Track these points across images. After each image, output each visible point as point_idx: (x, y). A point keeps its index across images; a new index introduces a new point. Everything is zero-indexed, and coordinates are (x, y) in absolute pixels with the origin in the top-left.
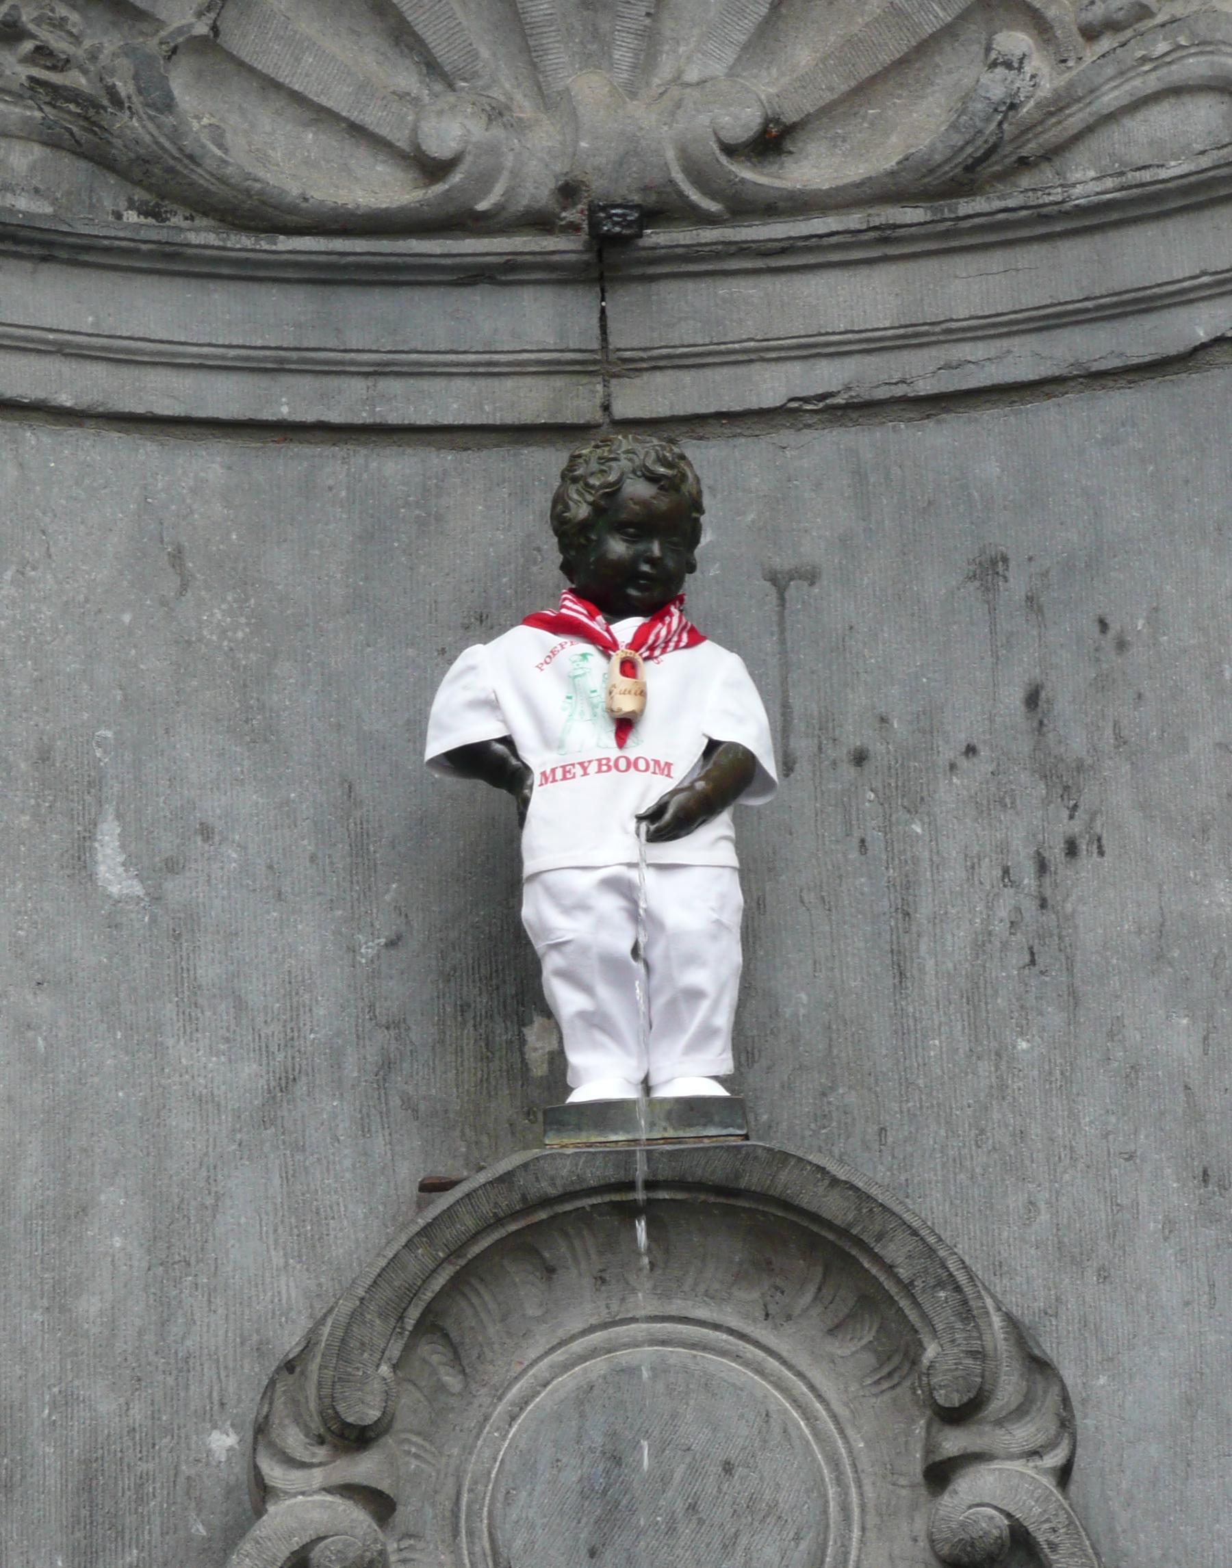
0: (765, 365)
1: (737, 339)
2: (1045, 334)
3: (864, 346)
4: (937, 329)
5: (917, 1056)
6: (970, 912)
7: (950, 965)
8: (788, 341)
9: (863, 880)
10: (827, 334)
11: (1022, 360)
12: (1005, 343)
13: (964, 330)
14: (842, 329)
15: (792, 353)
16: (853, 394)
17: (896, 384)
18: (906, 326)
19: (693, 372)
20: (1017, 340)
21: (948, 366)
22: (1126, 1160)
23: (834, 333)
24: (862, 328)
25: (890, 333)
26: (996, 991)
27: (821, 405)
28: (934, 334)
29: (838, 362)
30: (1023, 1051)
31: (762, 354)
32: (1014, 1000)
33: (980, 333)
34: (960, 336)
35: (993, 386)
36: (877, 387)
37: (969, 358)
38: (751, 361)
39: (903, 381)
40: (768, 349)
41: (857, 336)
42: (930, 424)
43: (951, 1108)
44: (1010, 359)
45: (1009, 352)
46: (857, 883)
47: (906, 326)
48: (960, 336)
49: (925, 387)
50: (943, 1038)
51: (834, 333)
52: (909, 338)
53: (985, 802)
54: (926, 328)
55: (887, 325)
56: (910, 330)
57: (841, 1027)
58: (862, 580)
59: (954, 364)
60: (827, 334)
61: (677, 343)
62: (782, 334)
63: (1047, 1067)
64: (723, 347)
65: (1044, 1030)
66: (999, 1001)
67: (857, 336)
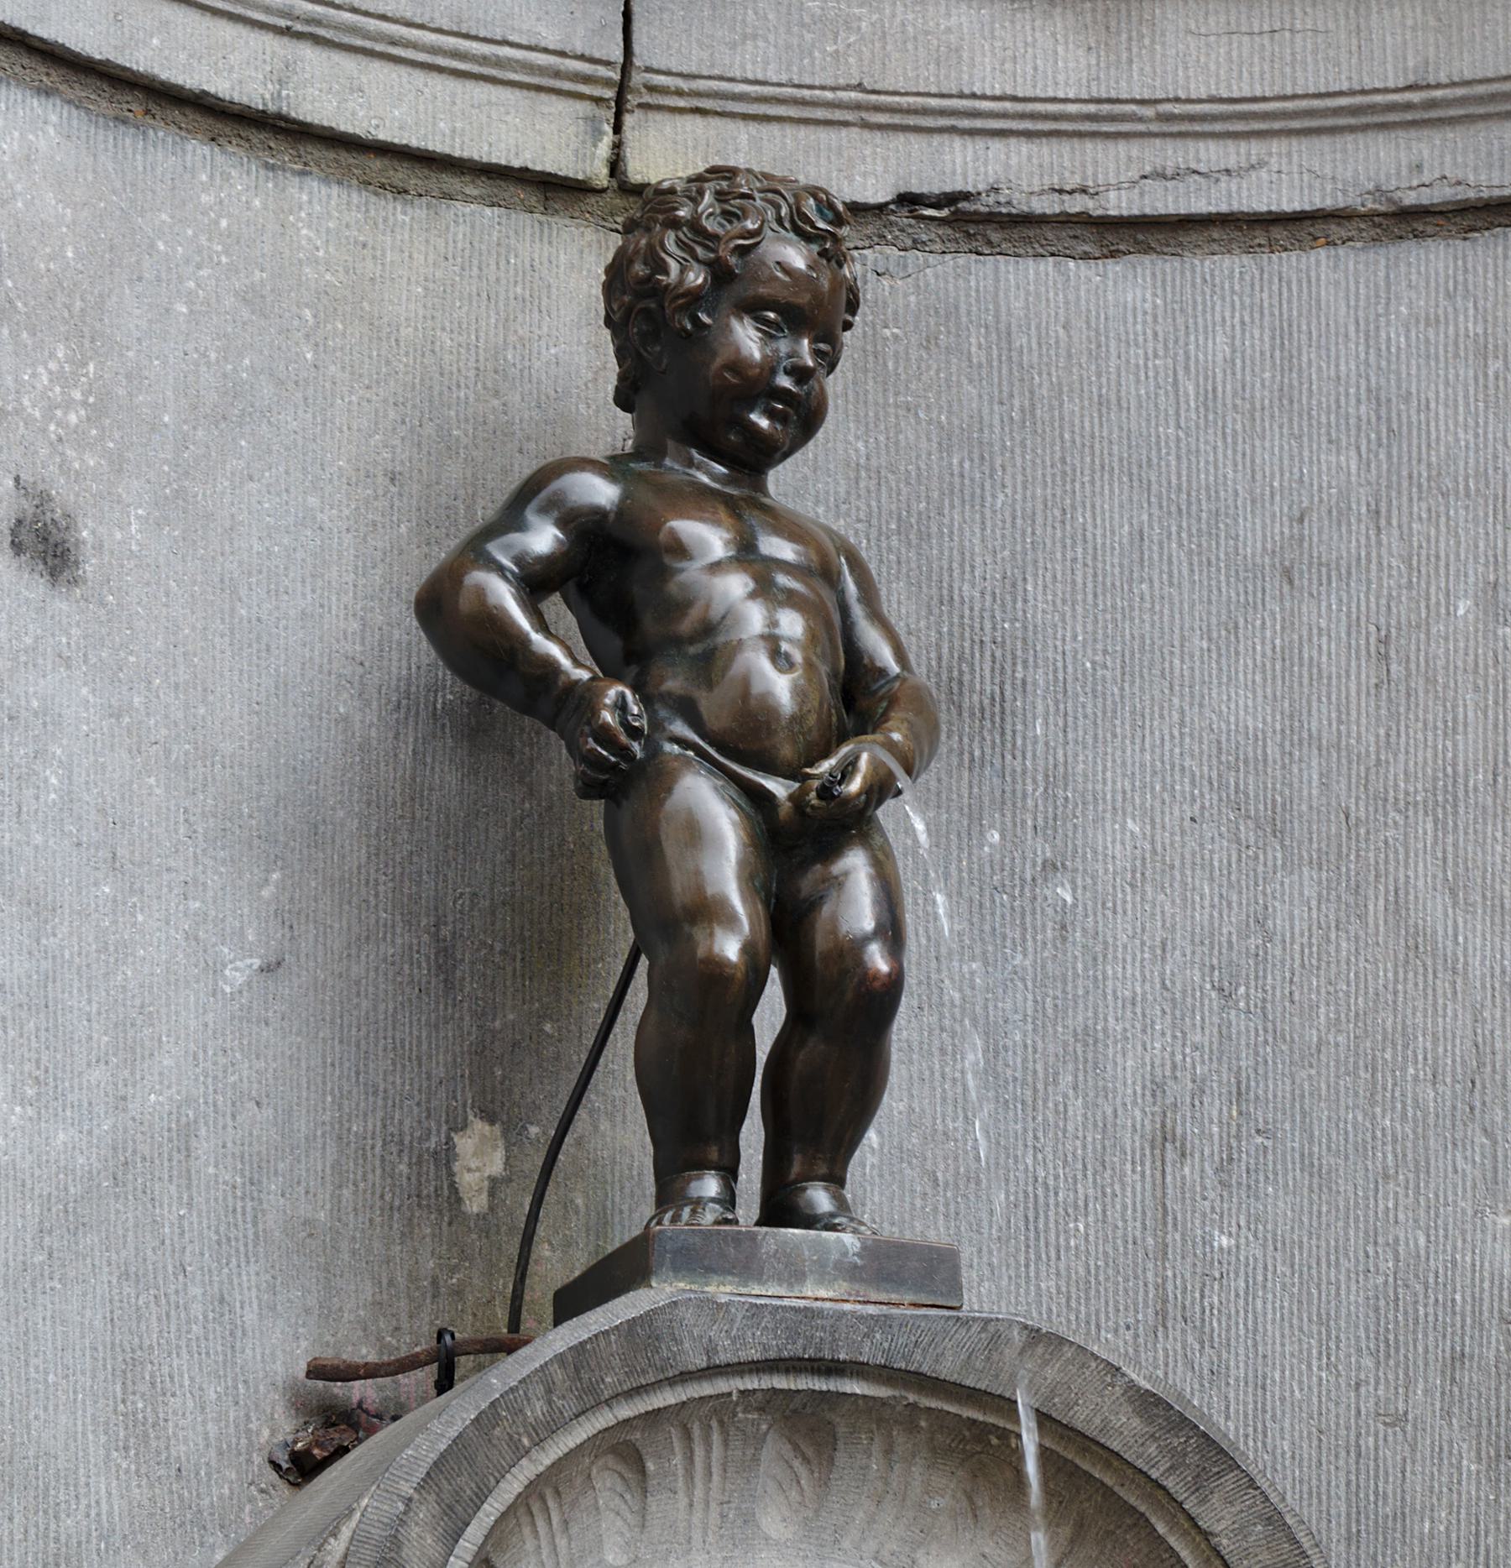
0: (867, 134)
1: (830, 82)
2: (1325, 142)
3: (1028, 125)
4: (1149, 112)
5: (1047, 1245)
6: (1144, 1031)
7: (1109, 1111)
8: (911, 100)
9: (974, 966)
10: (974, 96)
11: (1282, 179)
12: (1256, 148)
13: (1192, 118)
14: (998, 92)
15: (912, 121)
16: (1002, 200)
17: (1071, 193)
18: (1099, 101)
19: (753, 127)
20: (1275, 145)
21: (1161, 175)
22: (1385, 1424)
23: (984, 97)
24: (1029, 93)
25: (1072, 108)
26: (1183, 1155)
27: (945, 213)
28: (1141, 120)
29: (980, 143)
30: (1221, 1248)
31: (864, 115)
32: (1209, 1171)
33: (1218, 127)
34: (1185, 127)
35: (1232, 214)
36: (1042, 193)
37: (1193, 166)
38: (846, 124)
39: (1084, 191)
40: (877, 108)
41: (1019, 107)
42: (1114, 267)
43: (1098, 1327)
44: (1264, 174)
45: (1261, 164)
46: (965, 969)
47: (1099, 101)
48: (1185, 127)
49: (1118, 204)
50: (1091, 1219)
51: (984, 97)
52: (1101, 121)
53: (1177, 863)
54: (1133, 107)
55: (1071, 96)
56: (1106, 108)
57: (929, 1191)
58: (994, 496)
59: (1169, 172)
60: (974, 96)
61: (738, 74)
62: (901, 86)
63: (1260, 1278)
64: (806, 93)
65: (1257, 1220)
66: (1187, 1170)
67: (1019, 107)
